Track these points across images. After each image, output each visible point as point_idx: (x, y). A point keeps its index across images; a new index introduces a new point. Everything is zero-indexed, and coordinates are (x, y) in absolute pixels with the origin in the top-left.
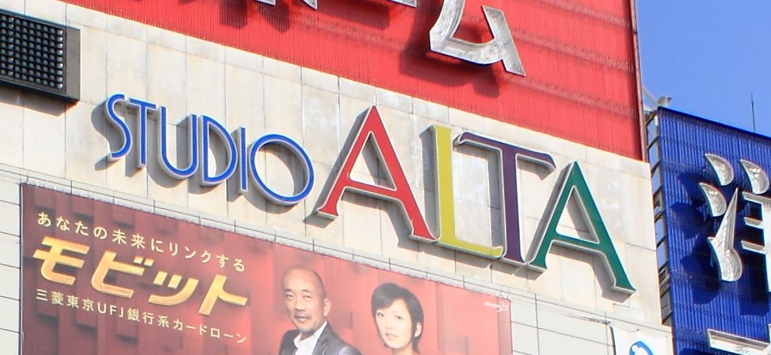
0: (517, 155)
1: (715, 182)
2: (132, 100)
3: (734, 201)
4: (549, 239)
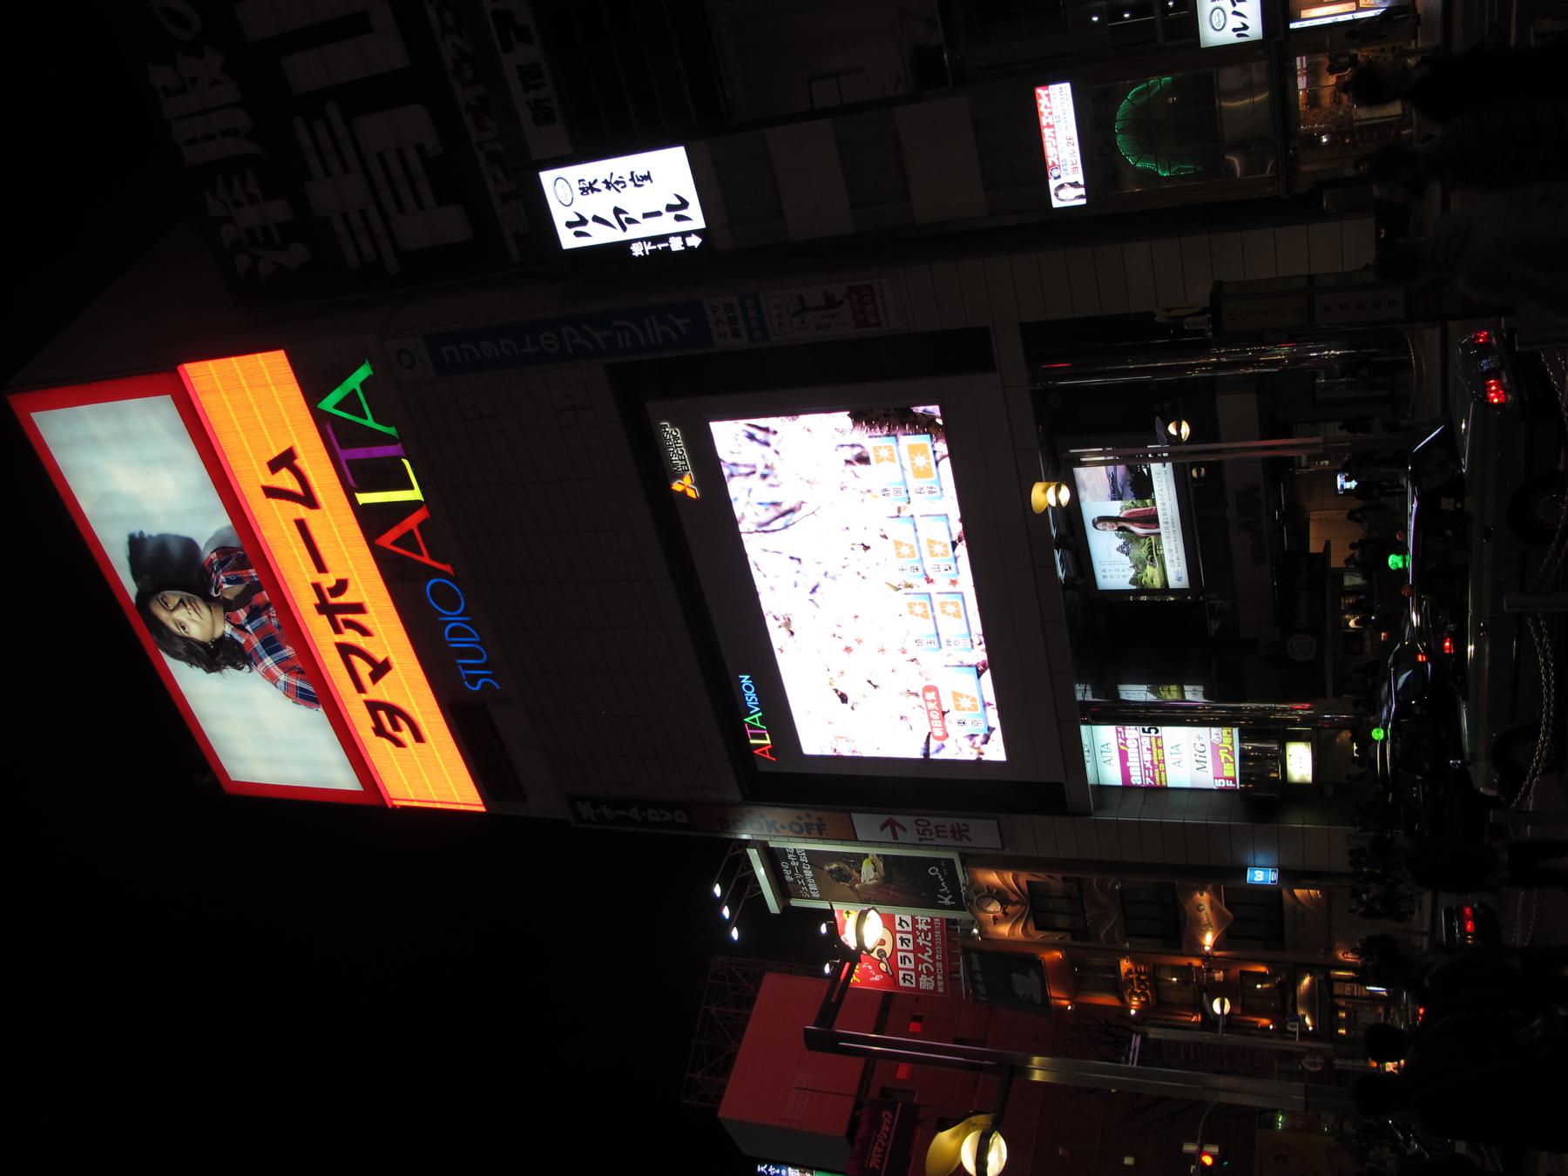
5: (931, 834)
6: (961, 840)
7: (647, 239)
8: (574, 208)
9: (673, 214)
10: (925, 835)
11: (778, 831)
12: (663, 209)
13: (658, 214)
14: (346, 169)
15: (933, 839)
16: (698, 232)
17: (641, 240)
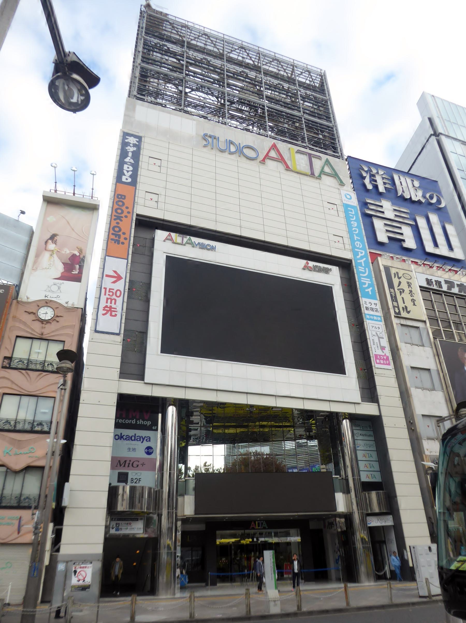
1: (363, 170)
3: (369, 174)
4: (322, 172)
5: (109, 295)
6: (103, 310)
7: (395, 294)
8: (402, 277)
9: (404, 307)
10: (109, 292)
11: (115, 219)
12: (405, 305)
13: (404, 303)
14: (396, 215)
15: (105, 295)
16: (399, 311)
17: (395, 293)
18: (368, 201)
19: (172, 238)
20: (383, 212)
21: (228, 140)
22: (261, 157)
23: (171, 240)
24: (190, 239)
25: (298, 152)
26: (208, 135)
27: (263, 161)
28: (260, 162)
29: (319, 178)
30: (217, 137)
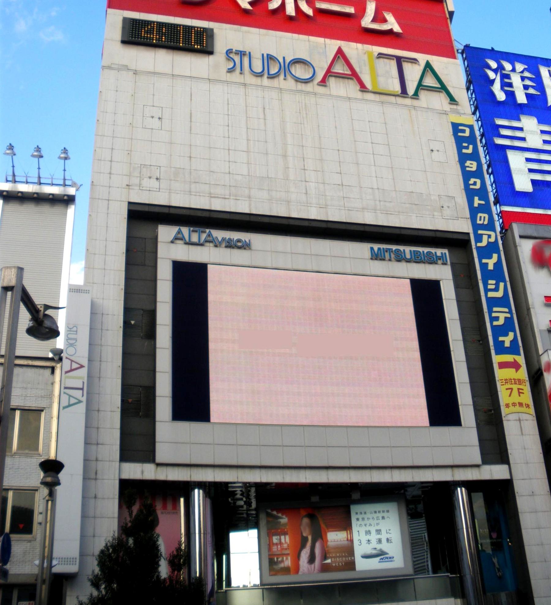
0: (402, 59)
1: (489, 67)
2: (236, 50)
3: (499, 74)
4: (420, 86)
18: (499, 122)
19: (183, 236)
20: (523, 139)
21: (265, 56)
22: (320, 76)
23: (182, 239)
24: (209, 235)
25: (381, 56)
26: (234, 50)
27: (323, 82)
28: (318, 84)
29: (416, 95)
30: (247, 53)
